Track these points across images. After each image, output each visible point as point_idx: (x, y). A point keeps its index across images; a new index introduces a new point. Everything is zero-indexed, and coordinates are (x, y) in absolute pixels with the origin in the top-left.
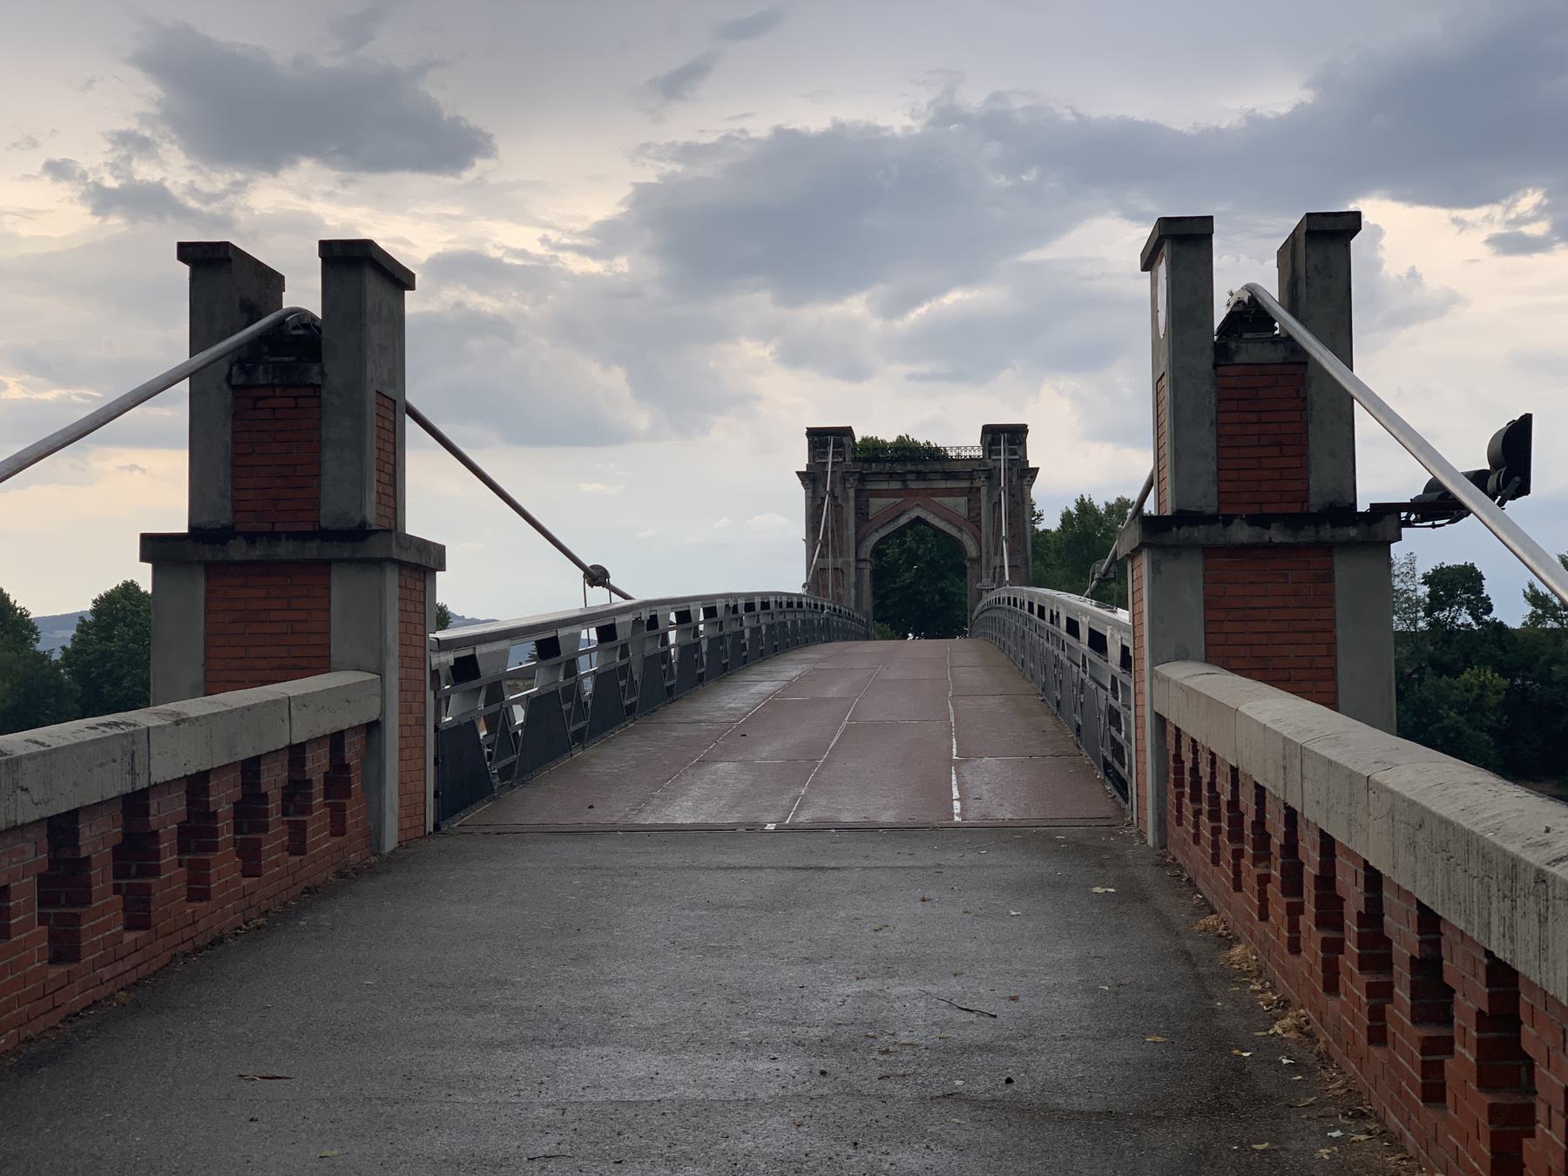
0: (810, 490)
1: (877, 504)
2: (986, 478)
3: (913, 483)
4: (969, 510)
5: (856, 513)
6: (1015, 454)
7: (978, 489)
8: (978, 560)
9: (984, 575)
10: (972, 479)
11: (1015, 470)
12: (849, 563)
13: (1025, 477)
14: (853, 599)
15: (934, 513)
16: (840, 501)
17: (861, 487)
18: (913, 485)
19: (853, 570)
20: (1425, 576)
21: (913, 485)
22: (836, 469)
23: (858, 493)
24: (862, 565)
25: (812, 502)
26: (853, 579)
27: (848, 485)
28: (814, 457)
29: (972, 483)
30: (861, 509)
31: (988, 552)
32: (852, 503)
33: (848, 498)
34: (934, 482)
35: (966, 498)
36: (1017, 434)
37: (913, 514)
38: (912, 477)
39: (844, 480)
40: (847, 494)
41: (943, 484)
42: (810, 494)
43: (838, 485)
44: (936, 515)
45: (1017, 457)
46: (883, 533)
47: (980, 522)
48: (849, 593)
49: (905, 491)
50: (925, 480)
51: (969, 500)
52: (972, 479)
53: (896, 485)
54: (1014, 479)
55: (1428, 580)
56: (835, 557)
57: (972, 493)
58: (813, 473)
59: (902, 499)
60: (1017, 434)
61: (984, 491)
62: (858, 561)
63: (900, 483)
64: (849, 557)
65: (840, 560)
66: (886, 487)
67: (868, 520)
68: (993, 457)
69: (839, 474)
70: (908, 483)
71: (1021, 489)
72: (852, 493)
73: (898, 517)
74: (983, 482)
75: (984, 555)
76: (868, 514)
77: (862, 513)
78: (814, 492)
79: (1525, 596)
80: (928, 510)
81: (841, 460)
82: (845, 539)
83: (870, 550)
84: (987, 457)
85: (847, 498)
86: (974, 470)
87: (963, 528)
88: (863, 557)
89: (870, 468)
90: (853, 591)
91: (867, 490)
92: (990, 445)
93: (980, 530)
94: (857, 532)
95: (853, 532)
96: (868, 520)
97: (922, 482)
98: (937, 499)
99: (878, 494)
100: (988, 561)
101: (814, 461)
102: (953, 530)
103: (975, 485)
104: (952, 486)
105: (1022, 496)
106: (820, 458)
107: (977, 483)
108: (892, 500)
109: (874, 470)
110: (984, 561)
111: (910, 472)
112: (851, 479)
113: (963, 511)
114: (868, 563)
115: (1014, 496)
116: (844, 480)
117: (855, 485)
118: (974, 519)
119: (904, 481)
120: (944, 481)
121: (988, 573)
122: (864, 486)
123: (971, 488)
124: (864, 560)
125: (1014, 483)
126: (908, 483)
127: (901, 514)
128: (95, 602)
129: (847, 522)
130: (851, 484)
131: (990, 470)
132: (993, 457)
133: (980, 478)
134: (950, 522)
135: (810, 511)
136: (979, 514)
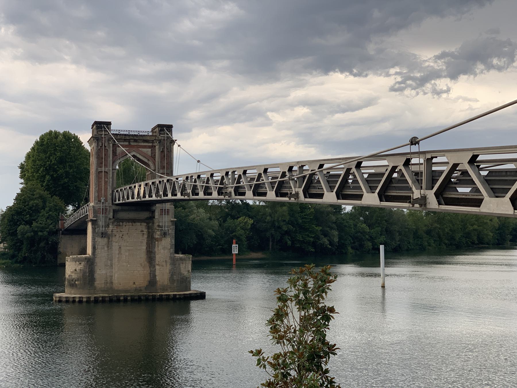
0: (96, 143)
3: (132, 143)
4: (152, 153)
7: (155, 146)
12: (110, 170)
13: (172, 143)
14: (111, 183)
15: (139, 154)
18: (132, 144)
21: (132, 144)
22: (106, 136)
26: (111, 176)
28: (98, 132)
31: (158, 168)
33: (110, 147)
36: (169, 128)
38: (132, 141)
41: (143, 144)
44: (140, 154)
48: (110, 181)
51: (152, 150)
53: (127, 143)
54: (168, 143)
57: (153, 147)
59: (128, 149)
60: (169, 128)
61: (157, 147)
63: (128, 143)
65: (107, 169)
70: (131, 143)
72: (111, 145)
78: (98, 144)
82: (108, 162)
90: (111, 180)
92: (160, 131)
93: (155, 160)
95: (112, 159)
98: (140, 149)
101: (98, 133)
106: (100, 132)
107: (155, 144)
111: (132, 139)
118: (153, 157)
119: (129, 142)
123: (152, 146)
126: (131, 143)
129: (109, 156)
131: (160, 140)
133: (156, 142)
136: (155, 155)
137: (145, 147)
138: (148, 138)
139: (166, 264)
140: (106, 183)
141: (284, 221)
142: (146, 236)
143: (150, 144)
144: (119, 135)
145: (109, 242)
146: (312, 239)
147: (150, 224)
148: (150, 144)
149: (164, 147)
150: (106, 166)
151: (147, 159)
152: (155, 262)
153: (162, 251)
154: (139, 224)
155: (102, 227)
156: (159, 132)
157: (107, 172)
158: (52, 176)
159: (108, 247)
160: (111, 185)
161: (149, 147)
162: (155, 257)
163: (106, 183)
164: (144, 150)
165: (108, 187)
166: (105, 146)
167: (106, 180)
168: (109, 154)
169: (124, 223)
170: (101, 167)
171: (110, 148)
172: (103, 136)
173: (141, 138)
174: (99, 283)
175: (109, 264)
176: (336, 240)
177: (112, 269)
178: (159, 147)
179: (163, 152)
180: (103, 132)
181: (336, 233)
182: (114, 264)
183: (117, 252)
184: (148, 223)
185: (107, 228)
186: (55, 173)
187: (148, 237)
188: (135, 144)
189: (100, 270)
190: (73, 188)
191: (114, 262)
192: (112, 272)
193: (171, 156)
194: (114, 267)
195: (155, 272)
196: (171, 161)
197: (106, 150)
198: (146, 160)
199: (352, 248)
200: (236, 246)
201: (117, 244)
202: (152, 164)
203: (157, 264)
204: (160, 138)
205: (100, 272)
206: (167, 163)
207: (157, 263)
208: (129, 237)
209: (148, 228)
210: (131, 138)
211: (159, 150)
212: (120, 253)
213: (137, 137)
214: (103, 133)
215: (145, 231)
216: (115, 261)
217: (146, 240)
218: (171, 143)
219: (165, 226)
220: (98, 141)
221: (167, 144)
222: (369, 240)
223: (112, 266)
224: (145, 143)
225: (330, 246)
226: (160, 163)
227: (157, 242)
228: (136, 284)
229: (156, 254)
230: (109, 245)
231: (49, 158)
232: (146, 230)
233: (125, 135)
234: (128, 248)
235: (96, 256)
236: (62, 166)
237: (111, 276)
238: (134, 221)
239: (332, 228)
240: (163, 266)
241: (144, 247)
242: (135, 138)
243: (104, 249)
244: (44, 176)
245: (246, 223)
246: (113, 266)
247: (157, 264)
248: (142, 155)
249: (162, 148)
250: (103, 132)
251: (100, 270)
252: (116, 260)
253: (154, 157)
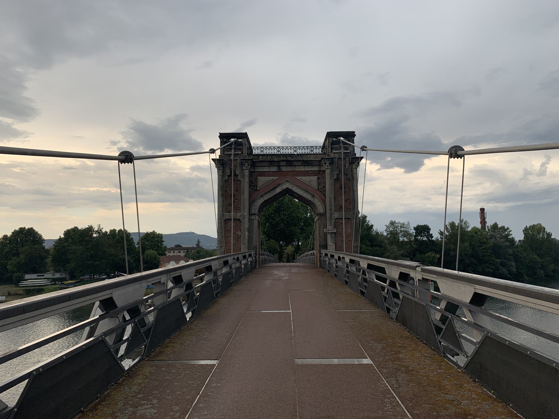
1: (262, 181)
2: (330, 164)
3: (285, 167)
4: (318, 184)
5: (250, 186)
6: (348, 150)
7: (324, 171)
8: (323, 215)
9: (328, 223)
10: (320, 165)
11: (347, 159)
12: (244, 216)
13: (354, 163)
14: (247, 238)
15: (297, 186)
16: (239, 178)
17: (253, 170)
18: (284, 169)
19: (247, 220)
20: (414, 228)
21: (284, 169)
22: (237, 158)
23: (251, 174)
24: (253, 217)
25: (222, 178)
26: (247, 226)
27: (244, 168)
28: (224, 151)
29: (320, 168)
30: (252, 183)
31: (331, 210)
32: (247, 180)
33: (244, 176)
34: (297, 167)
35: (317, 177)
37: (284, 187)
38: (282, 164)
39: (242, 164)
40: (244, 173)
41: (302, 169)
42: (221, 173)
43: (238, 168)
44: (299, 187)
45: (349, 151)
46: (266, 197)
47: (325, 191)
48: (244, 235)
49: (279, 173)
50: (291, 166)
52: (320, 165)
53: (274, 169)
54: (347, 165)
55: (415, 229)
56: (235, 212)
57: (320, 174)
58: (223, 160)
59: (277, 178)
61: (328, 172)
62: (250, 214)
63: (276, 168)
64: (245, 212)
65: (239, 214)
66: (268, 170)
67: (257, 190)
68: (334, 151)
69: (239, 161)
70: (282, 167)
71: (352, 170)
72: (247, 173)
73: (275, 188)
74: (328, 166)
75: (328, 211)
76: (257, 186)
77: (253, 186)
78: (223, 172)
79: (439, 233)
80: (293, 184)
81: (240, 152)
82: (242, 201)
83: (258, 208)
84: (330, 151)
85: (244, 176)
86: (322, 158)
87: (315, 195)
88: (253, 212)
89: (258, 159)
90: (247, 233)
91: (256, 172)
93: (325, 196)
94: (250, 197)
96: (257, 190)
97: (290, 167)
99: (263, 174)
100: (331, 214)
101: (224, 154)
102: (308, 196)
103: (322, 169)
104: (308, 170)
105: (352, 175)
106: (227, 152)
108: (271, 178)
109: (260, 160)
110: (328, 215)
111: (282, 161)
112: (246, 164)
114: (257, 216)
115: (347, 175)
116: (242, 164)
117: (248, 168)
118: (322, 190)
119: (279, 167)
120: (303, 167)
121: (331, 223)
122: (255, 169)
123: (319, 171)
124: (254, 214)
125: (347, 167)
126: (282, 167)
127: (277, 187)
128: (65, 231)
129: (243, 190)
130: (246, 167)
131: (332, 158)
132: (334, 151)
133: (326, 163)
134: (307, 191)
135: (221, 183)
136: (324, 187)
137: (306, 174)
138: (312, 158)
140: (238, 238)
141: (466, 255)
143: (316, 169)
144: (262, 155)
146: (491, 271)
148: (316, 169)
149: (340, 171)
150: (237, 209)
151: (311, 194)
156: (330, 146)
157: (239, 220)
158: (271, 223)
160: (246, 242)
161: (314, 173)
163: (238, 238)
165: (242, 246)
166: (236, 175)
167: (239, 233)
168: (243, 189)
170: (229, 212)
171: (244, 178)
172: (232, 158)
173: (300, 158)
176: (514, 270)
178: (331, 173)
179: (338, 179)
180: (233, 150)
181: (513, 264)
186: (273, 221)
188: (289, 169)
190: (288, 232)
193: (353, 187)
196: (354, 195)
197: (239, 182)
198: (309, 197)
199: (527, 275)
200: (432, 284)
202: (320, 202)
204: (332, 155)
206: (346, 201)
210: (282, 158)
211: (331, 178)
213: (292, 157)
214: (232, 152)
218: (352, 163)
220: (223, 167)
221: (345, 166)
222: (541, 269)
224: (306, 167)
225: (509, 275)
226: (333, 201)
231: (268, 210)
233: (272, 155)
236: (277, 215)
239: (509, 260)
242: (289, 158)
244: (265, 224)
245: (433, 257)
248: (301, 189)
249: (336, 173)
250: (233, 150)
253: (324, 189)
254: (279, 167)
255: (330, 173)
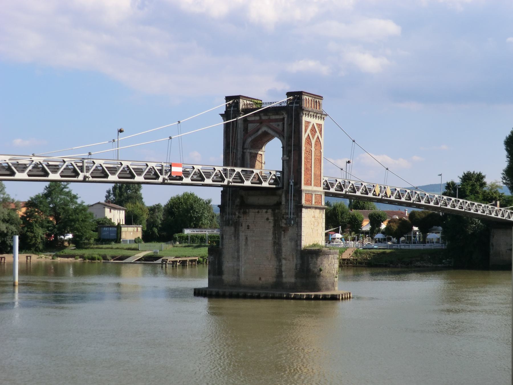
3: (264, 117)
21: (264, 118)
35: (282, 123)
113: (280, 128)
119: (260, 116)
139: (293, 258)
142: (272, 225)
145: (235, 231)
147: (277, 211)
152: (281, 255)
153: (289, 243)
154: (264, 211)
155: (229, 215)
159: (235, 237)
162: (281, 250)
164: (274, 125)
169: (251, 210)
174: (227, 277)
175: (236, 256)
177: (239, 261)
182: (240, 256)
183: (244, 243)
184: (273, 210)
185: (233, 216)
187: (275, 226)
189: (228, 262)
191: (240, 254)
192: (239, 265)
194: (240, 260)
195: (282, 267)
201: (244, 234)
203: (284, 259)
205: (228, 264)
207: (283, 256)
208: (255, 226)
209: (274, 215)
212: (246, 244)
215: (271, 219)
216: (242, 253)
217: (272, 230)
219: (291, 213)
223: (238, 257)
227: (283, 232)
228: (263, 279)
229: (282, 246)
230: (236, 235)
232: (273, 218)
234: (254, 238)
235: (224, 246)
237: (238, 270)
238: (260, 207)
240: (289, 260)
241: (270, 238)
243: (231, 239)
246: (240, 258)
247: (283, 258)
251: (228, 262)
252: (243, 252)
254: (260, 116)
255: (287, 120)
